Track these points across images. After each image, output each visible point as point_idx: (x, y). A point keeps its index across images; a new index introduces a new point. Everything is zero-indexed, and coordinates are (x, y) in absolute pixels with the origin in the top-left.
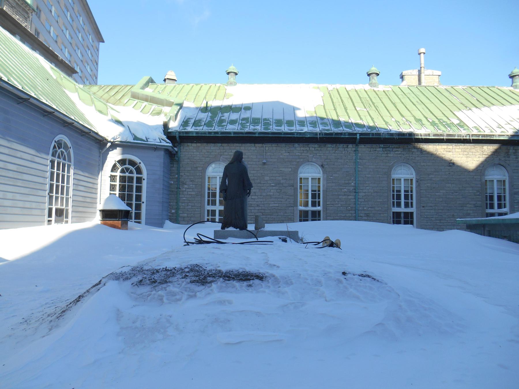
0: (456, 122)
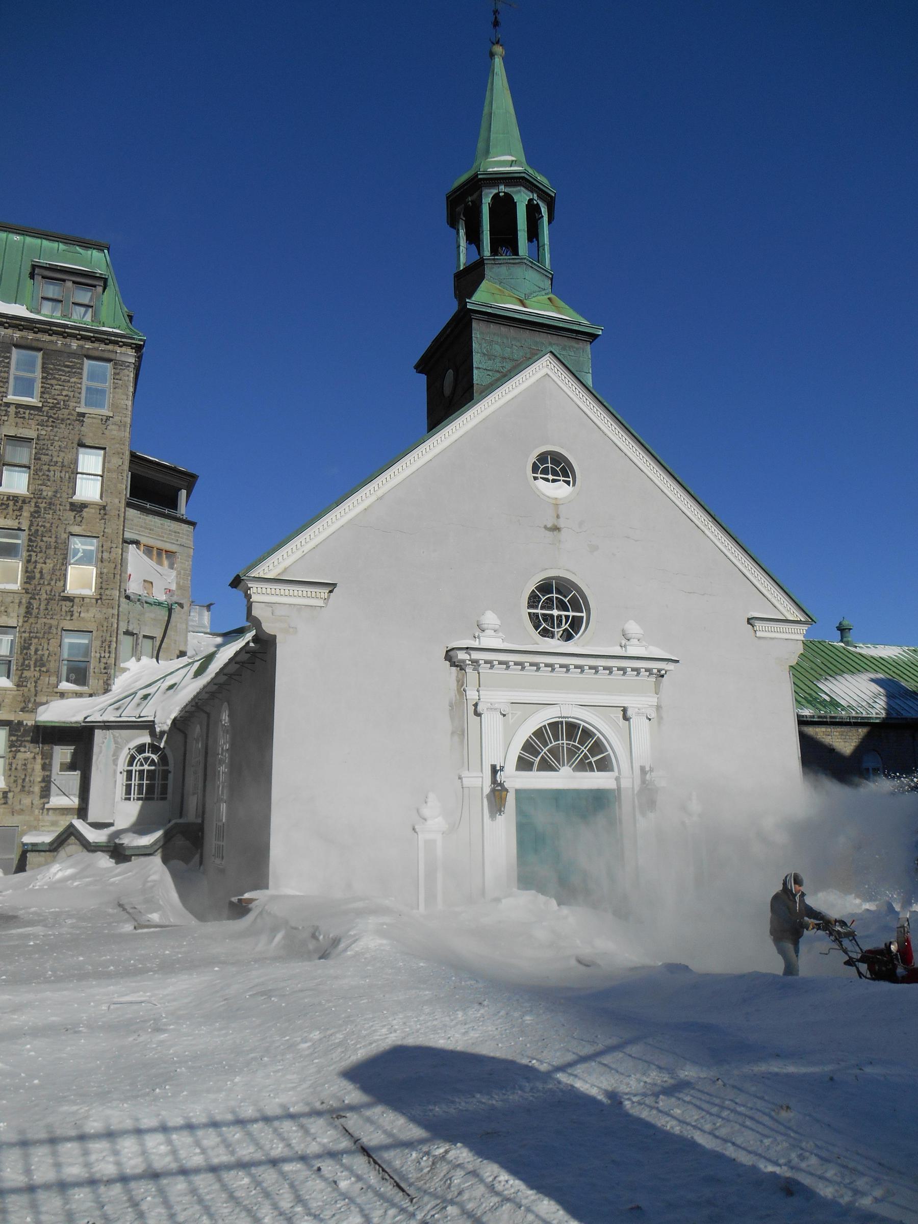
0: (827, 698)
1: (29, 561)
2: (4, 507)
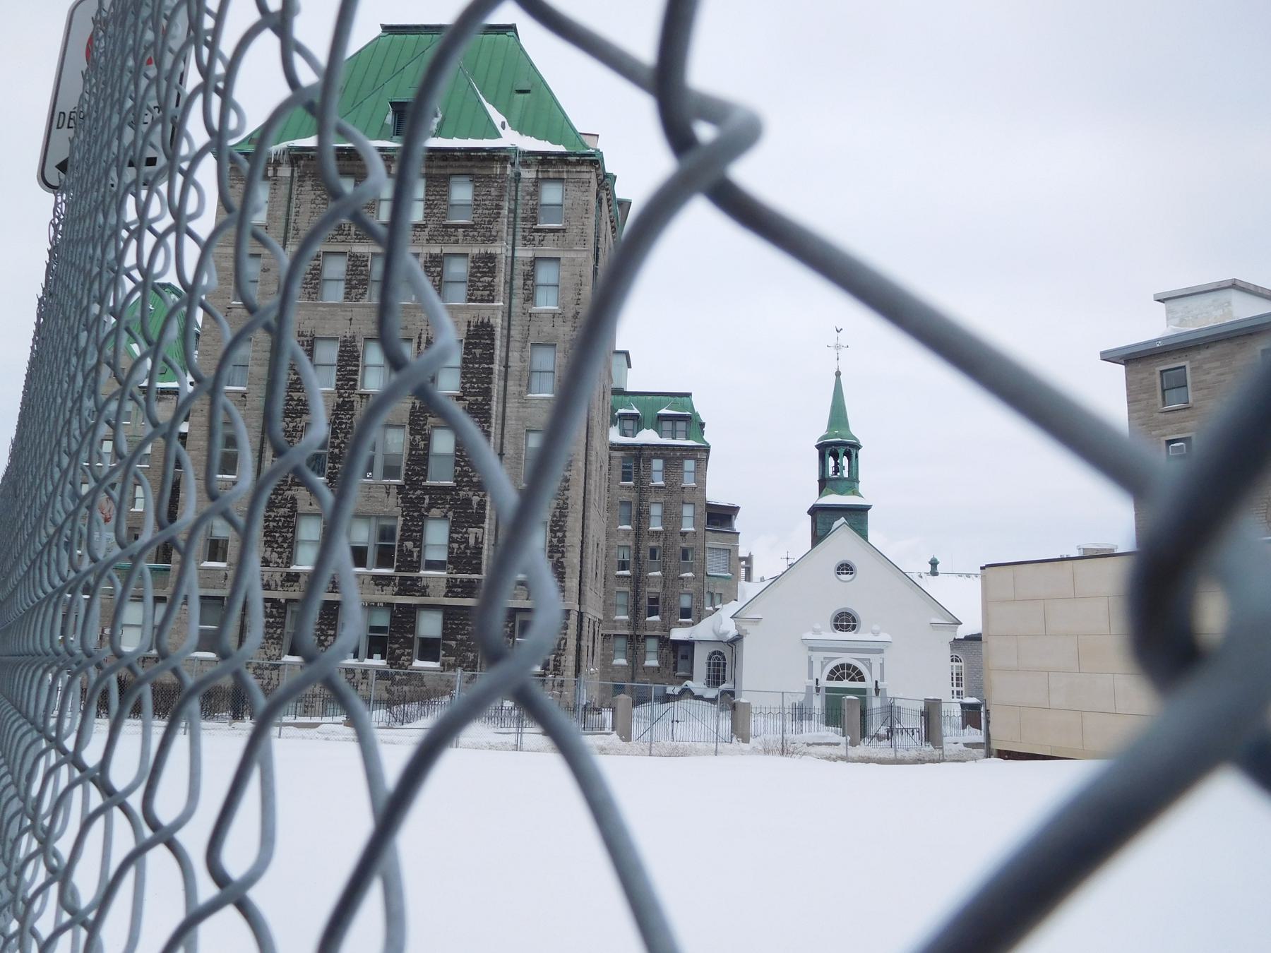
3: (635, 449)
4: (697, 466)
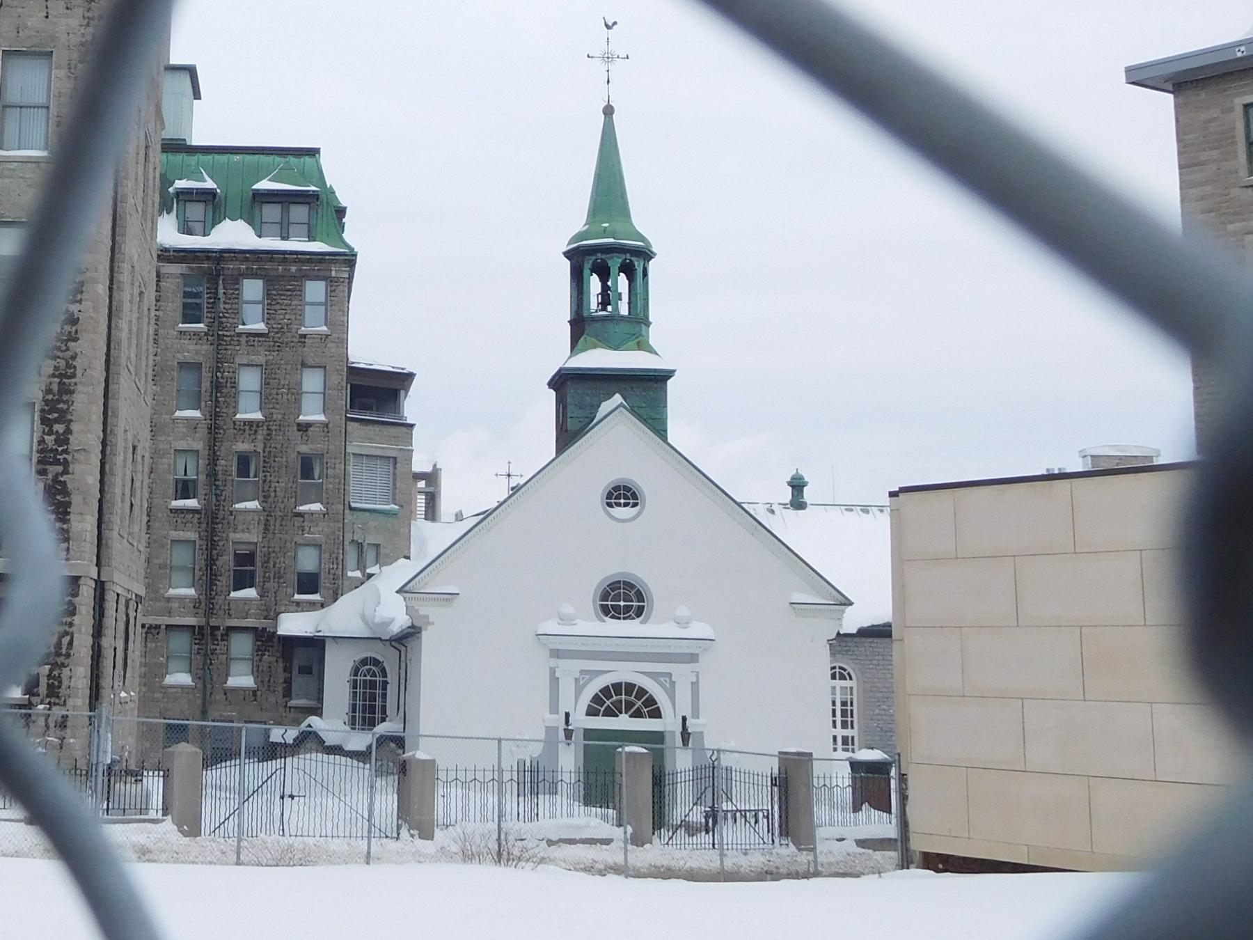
1: (265, 481)
2: (241, 432)
3: (208, 258)
4: (330, 293)
